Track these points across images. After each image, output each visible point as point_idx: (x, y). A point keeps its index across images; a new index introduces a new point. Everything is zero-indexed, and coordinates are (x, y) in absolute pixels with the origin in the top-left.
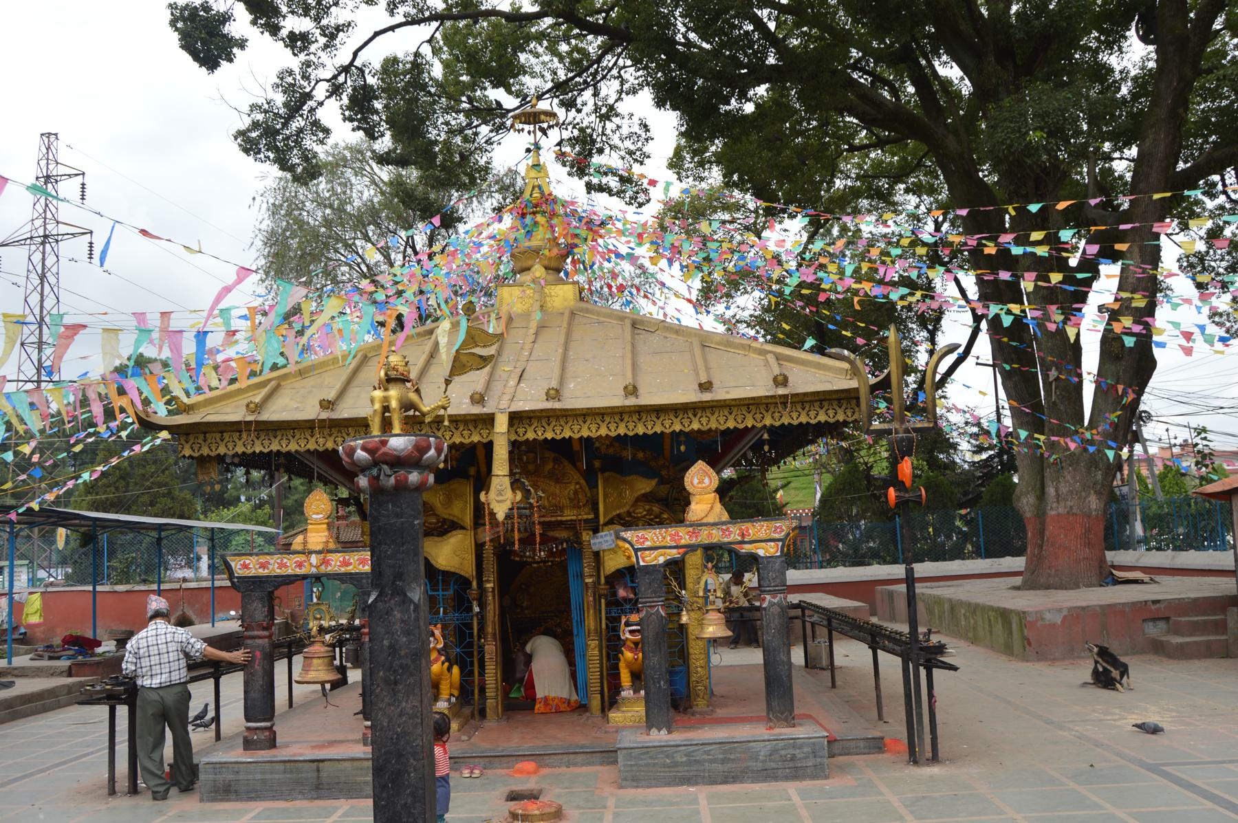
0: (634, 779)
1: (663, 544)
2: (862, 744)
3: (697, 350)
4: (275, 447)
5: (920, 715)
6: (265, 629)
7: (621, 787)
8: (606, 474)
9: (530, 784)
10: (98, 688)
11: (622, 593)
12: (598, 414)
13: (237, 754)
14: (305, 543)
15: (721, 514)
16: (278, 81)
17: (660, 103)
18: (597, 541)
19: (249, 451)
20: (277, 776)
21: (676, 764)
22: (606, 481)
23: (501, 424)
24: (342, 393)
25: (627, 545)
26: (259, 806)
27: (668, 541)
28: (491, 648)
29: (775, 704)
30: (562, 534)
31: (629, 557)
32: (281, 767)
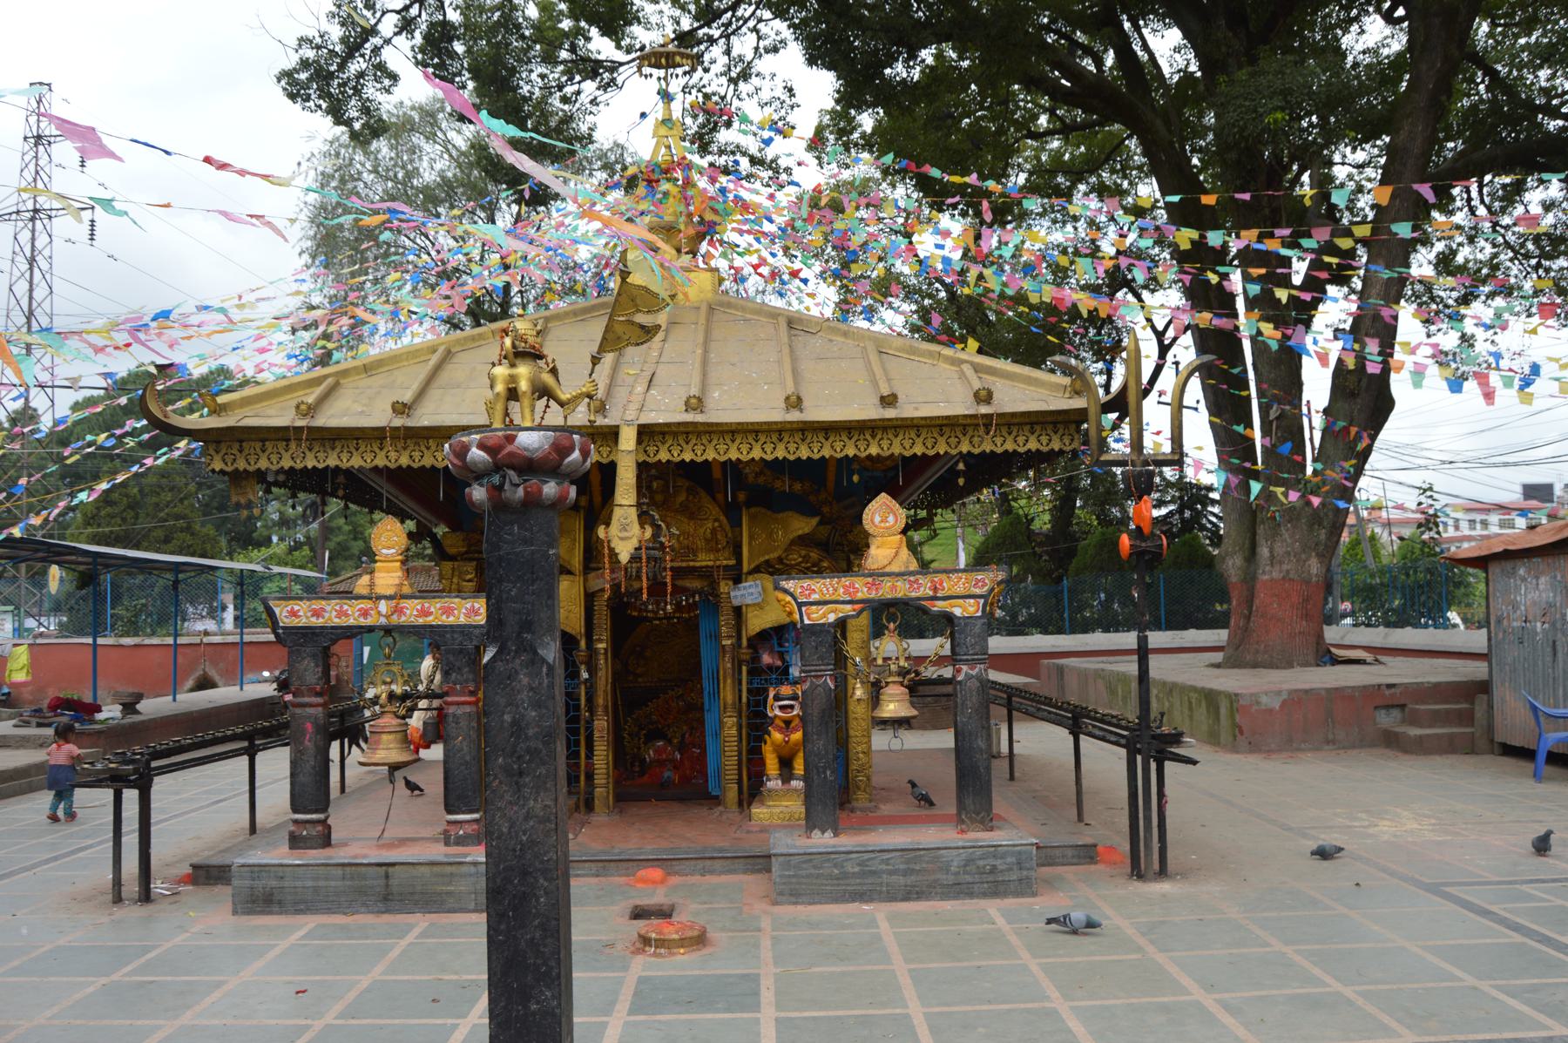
0: (794, 895)
1: (834, 598)
2: (1069, 852)
3: (873, 357)
4: (332, 462)
5: (1148, 819)
6: (318, 694)
7: (775, 903)
8: (753, 510)
9: (657, 897)
10: (99, 766)
11: (766, 659)
12: (751, 431)
13: (278, 854)
14: (372, 585)
15: (908, 562)
16: (334, 9)
17: (811, 61)
18: (738, 593)
19: (299, 466)
20: (333, 883)
21: (845, 876)
22: (752, 518)
23: (628, 440)
24: (421, 394)
25: (789, 598)
26: (310, 922)
28: (601, 724)
29: (969, 802)
30: (695, 584)
31: (790, 614)
32: (339, 871)
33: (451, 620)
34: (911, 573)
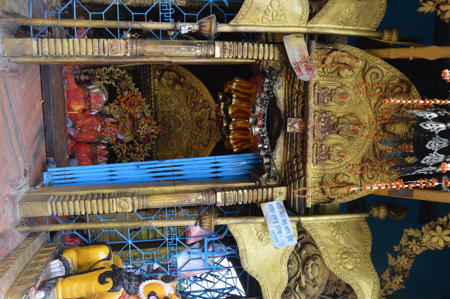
18: (277, 211)
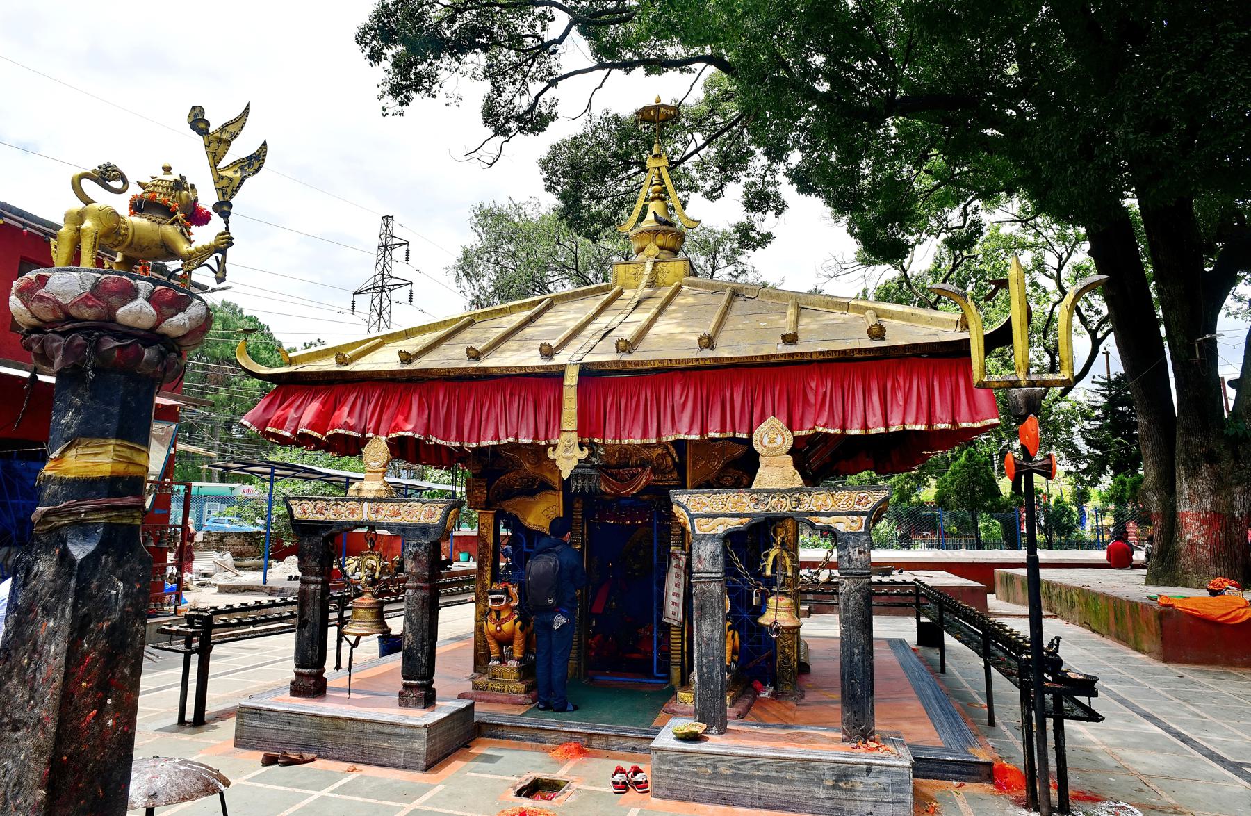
1: (723, 511)
6: (316, 575)
14: (358, 491)
20: (304, 730)
21: (717, 775)
25: (682, 510)
27: (729, 509)
33: (414, 520)
34: (795, 490)
